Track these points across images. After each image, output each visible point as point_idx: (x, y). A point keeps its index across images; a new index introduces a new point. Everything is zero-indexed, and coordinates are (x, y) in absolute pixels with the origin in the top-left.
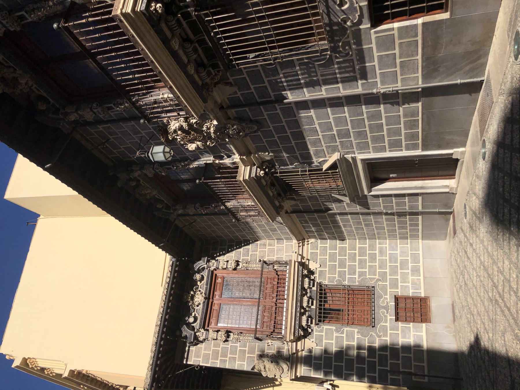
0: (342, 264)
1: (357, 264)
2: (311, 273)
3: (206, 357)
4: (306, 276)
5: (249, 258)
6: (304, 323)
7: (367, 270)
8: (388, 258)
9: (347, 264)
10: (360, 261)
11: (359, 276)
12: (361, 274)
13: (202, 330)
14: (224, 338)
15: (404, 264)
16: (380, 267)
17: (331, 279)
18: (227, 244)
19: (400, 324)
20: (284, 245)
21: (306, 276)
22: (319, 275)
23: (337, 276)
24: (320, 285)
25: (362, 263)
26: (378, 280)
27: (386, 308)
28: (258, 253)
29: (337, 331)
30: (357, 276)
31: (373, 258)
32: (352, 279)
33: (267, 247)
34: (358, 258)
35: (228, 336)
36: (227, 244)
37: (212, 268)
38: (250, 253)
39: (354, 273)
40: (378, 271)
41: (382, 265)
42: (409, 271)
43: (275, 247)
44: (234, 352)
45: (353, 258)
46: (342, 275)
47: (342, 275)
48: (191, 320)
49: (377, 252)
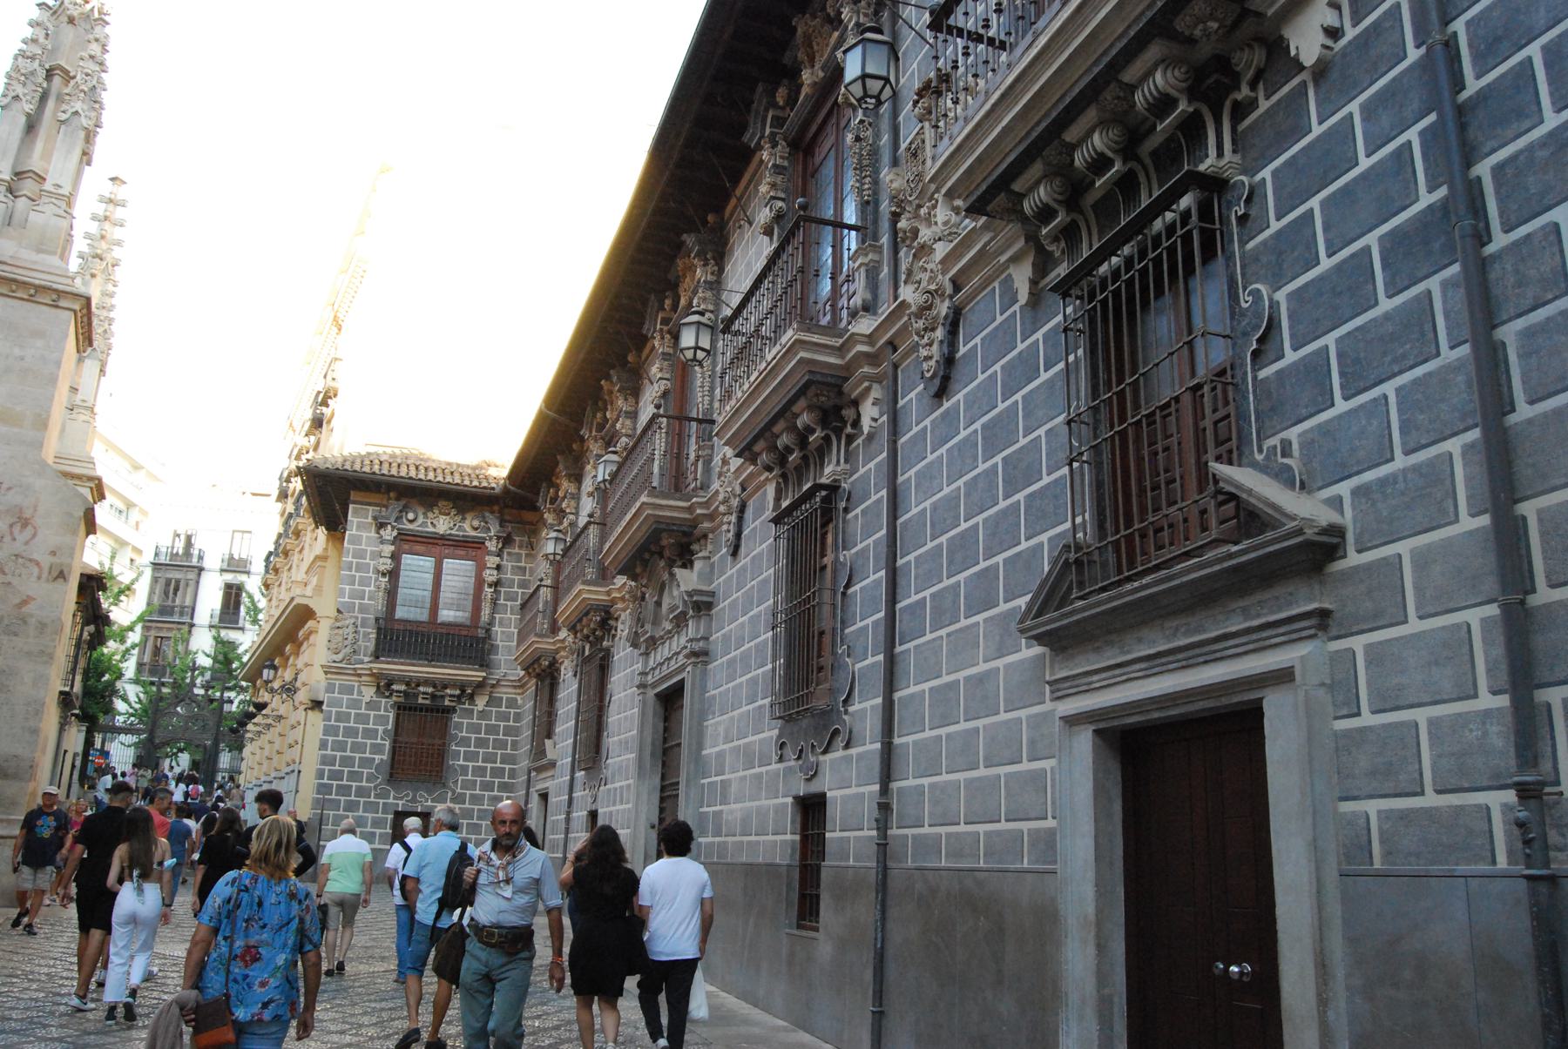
0: (481, 743)
2: (471, 697)
3: (356, 540)
4: (463, 691)
6: (394, 687)
12: (464, 770)
13: (395, 533)
14: (382, 568)
17: (459, 726)
19: (390, 817)
21: (463, 691)
24: (450, 711)
25: (480, 771)
26: (454, 792)
27: (414, 800)
29: (385, 731)
32: (458, 758)
35: (384, 575)
37: (488, 543)
44: (364, 582)
45: (489, 758)
46: (465, 742)
47: (465, 742)
48: (411, 516)
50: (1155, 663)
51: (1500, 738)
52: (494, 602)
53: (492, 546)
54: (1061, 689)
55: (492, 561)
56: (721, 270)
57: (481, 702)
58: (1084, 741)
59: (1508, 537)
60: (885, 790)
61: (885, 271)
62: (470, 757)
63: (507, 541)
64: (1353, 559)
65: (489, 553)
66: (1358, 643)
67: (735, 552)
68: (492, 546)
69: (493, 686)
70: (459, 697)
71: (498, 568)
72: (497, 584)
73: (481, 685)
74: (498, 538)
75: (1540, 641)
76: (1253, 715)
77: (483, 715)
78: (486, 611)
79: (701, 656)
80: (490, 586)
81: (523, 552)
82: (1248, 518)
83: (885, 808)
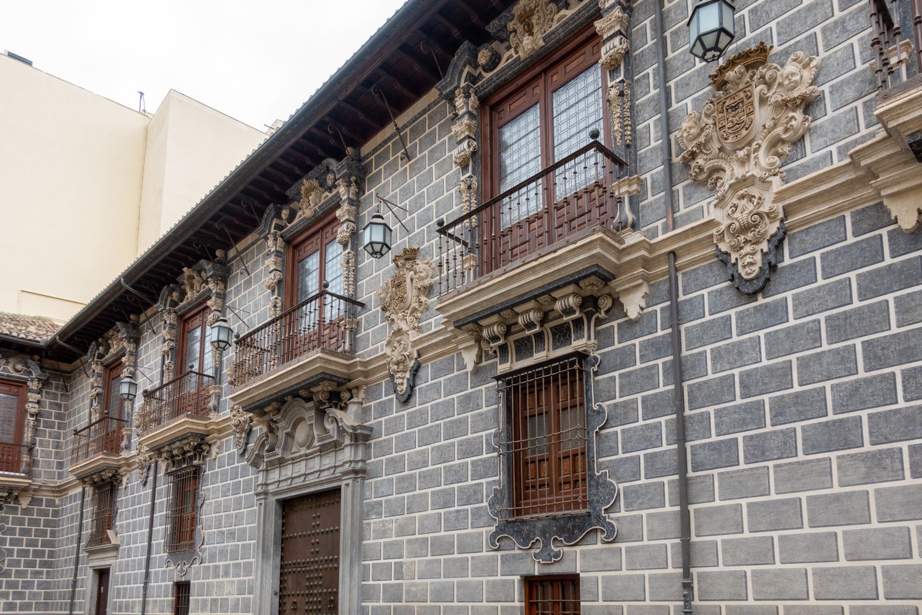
0: (24, 532)
1: (24, 547)
2: (16, 499)
5: (41, 428)
7: (15, 558)
8: (29, 579)
9: (25, 538)
10: (27, 551)
11: (7, 550)
12: (10, 552)
15: (20, 595)
16: (17, 571)
18: (63, 403)
20: (55, 470)
21: (10, 494)
22: (12, 507)
23: (10, 526)
28: (47, 439)
30: (8, 547)
31: (31, 564)
33: (54, 450)
34: (32, 549)
36: (63, 403)
38: (47, 430)
39: (11, 544)
40: (14, 569)
41: (19, 574)
42: (10, 600)
43: (53, 459)
45: (31, 543)
49: (37, 569)
52: (35, 430)
53: (34, 385)
55: (33, 397)
57: (24, 503)
62: (14, 542)
63: (45, 383)
65: (31, 391)
68: (34, 385)
69: (35, 490)
70: (6, 498)
71: (38, 402)
72: (37, 415)
73: (25, 490)
74: (39, 380)
77: (26, 511)
78: (28, 435)
80: (32, 415)
81: (59, 393)
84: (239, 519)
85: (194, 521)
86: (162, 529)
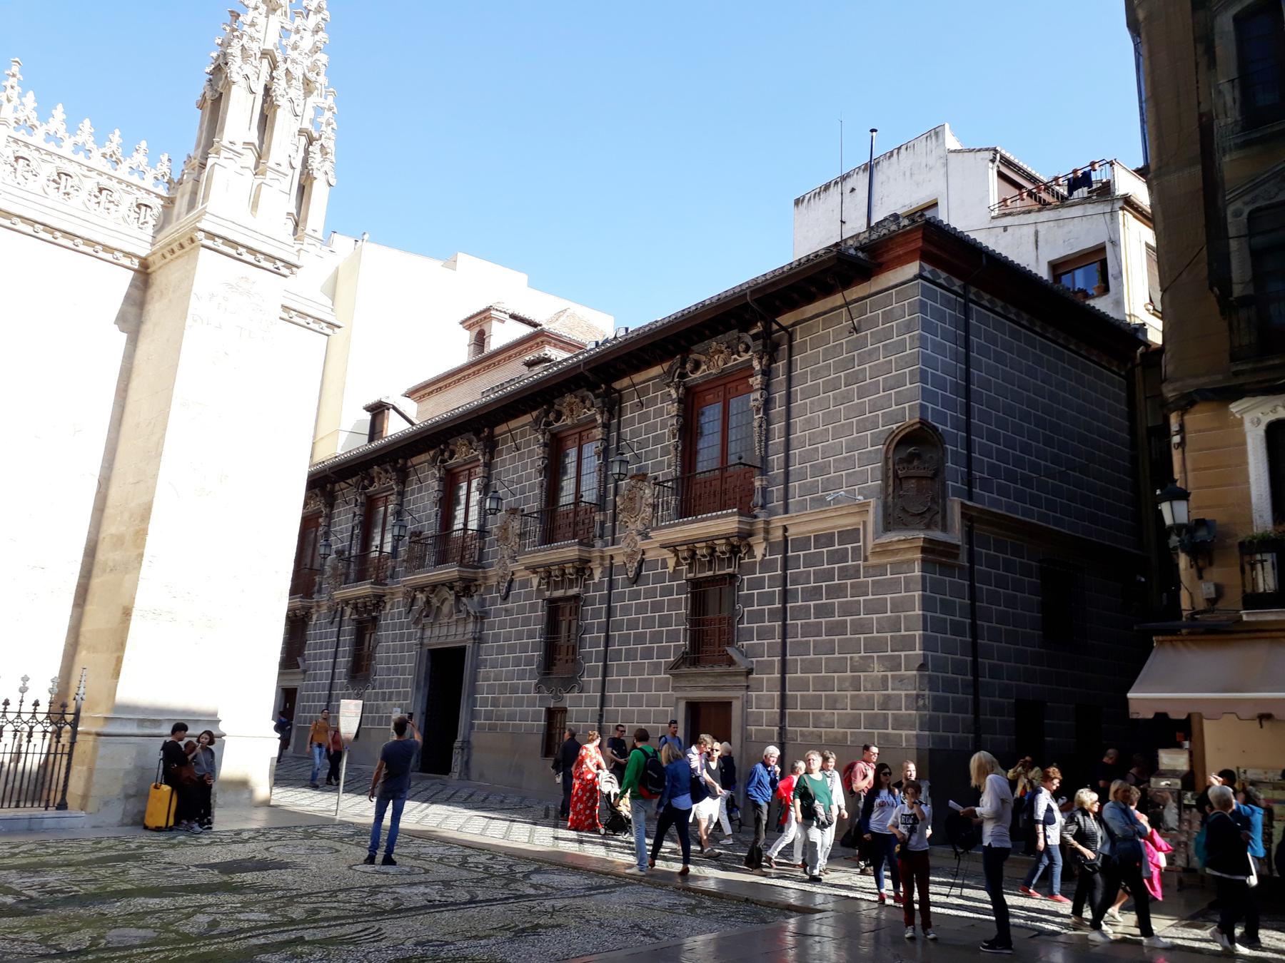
50: (706, 688)
51: (777, 717)
54: (674, 689)
56: (492, 458)
58: (682, 705)
59: (783, 680)
60: (601, 710)
61: (609, 524)
64: (754, 676)
66: (754, 694)
67: (505, 598)
75: (788, 700)
76: (730, 704)
79: (479, 639)
82: (731, 662)
83: (601, 716)
84: (402, 660)
85: (371, 657)
86: (344, 660)
